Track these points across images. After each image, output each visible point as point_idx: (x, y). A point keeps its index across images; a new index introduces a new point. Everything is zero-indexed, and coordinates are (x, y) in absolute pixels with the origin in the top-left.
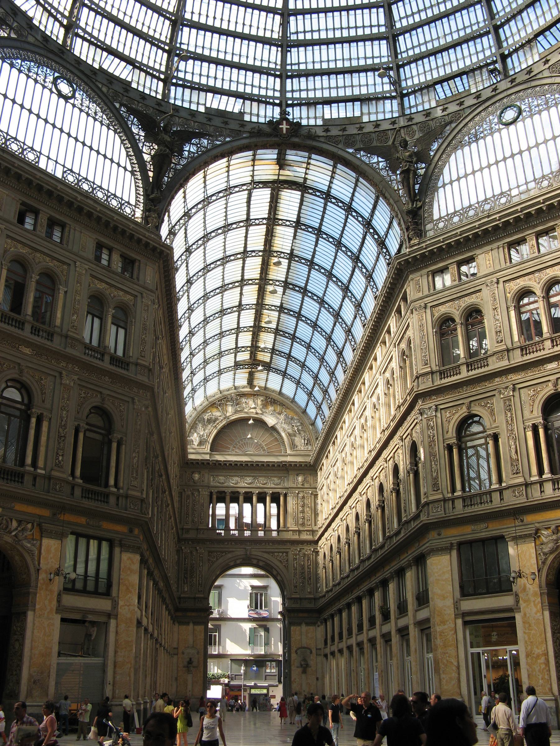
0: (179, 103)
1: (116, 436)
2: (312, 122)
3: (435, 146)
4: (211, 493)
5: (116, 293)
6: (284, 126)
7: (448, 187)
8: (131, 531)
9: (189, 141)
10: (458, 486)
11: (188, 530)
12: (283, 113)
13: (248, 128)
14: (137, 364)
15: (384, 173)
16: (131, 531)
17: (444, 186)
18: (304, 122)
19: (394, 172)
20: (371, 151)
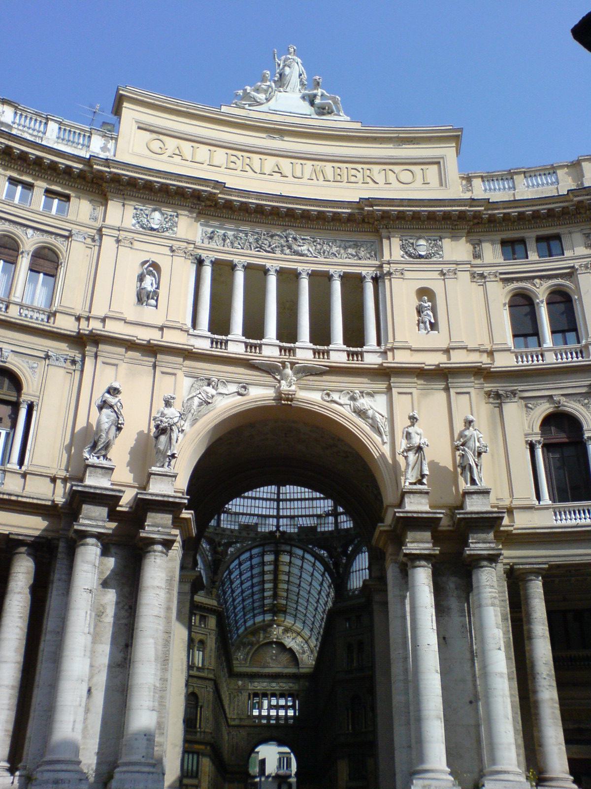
0: (225, 526)
1: (200, 704)
2: (292, 531)
3: (350, 549)
4: (249, 695)
5: (198, 635)
6: (278, 534)
7: (354, 573)
8: (206, 748)
9: (231, 546)
10: (350, 728)
11: (234, 719)
12: (278, 526)
13: (259, 536)
14: (208, 669)
15: (327, 560)
16: (206, 748)
17: (353, 572)
18: (288, 531)
19: (331, 560)
20: (321, 548)
